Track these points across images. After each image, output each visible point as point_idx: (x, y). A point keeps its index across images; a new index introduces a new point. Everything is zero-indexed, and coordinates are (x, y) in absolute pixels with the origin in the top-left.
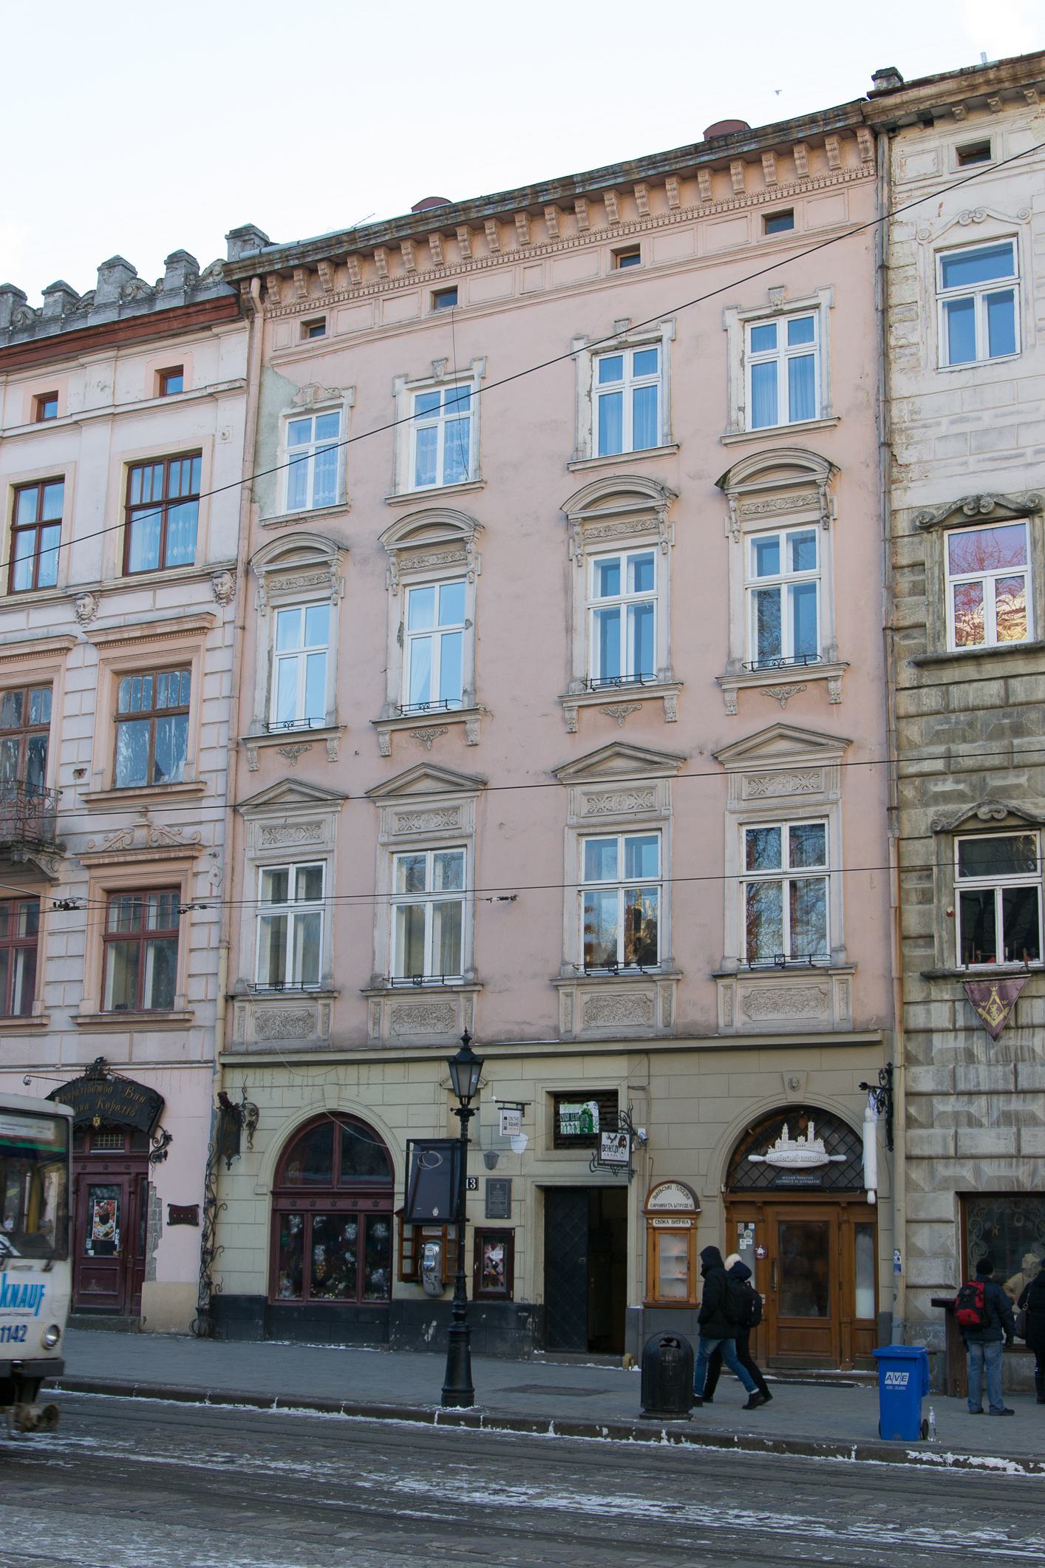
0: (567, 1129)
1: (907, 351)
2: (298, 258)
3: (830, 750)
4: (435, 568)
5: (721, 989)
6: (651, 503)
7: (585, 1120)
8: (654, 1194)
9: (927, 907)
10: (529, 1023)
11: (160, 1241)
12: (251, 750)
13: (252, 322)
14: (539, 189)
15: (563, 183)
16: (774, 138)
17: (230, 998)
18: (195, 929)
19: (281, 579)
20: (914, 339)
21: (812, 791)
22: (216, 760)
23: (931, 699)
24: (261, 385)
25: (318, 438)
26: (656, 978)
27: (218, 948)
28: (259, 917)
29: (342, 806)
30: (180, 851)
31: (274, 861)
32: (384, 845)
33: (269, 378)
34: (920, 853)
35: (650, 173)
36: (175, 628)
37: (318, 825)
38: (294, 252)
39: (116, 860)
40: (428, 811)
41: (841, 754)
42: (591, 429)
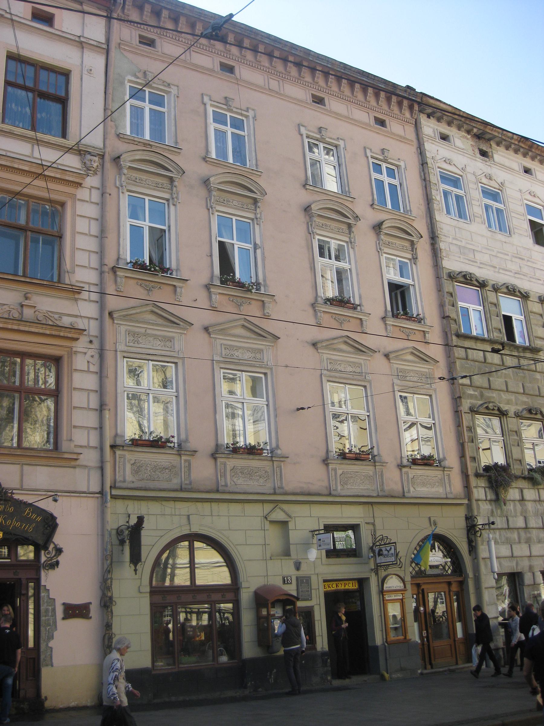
0: (339, 546)
6: (350, 221)
11: (55, 634)
14: (294, 47)
16: (391, 88)
19: (136, 175)
30: (70, 332)
35: (342, 71)
36: (58, 176)
37: (170, 339)
39: (10, 326)
40: (243, 348)
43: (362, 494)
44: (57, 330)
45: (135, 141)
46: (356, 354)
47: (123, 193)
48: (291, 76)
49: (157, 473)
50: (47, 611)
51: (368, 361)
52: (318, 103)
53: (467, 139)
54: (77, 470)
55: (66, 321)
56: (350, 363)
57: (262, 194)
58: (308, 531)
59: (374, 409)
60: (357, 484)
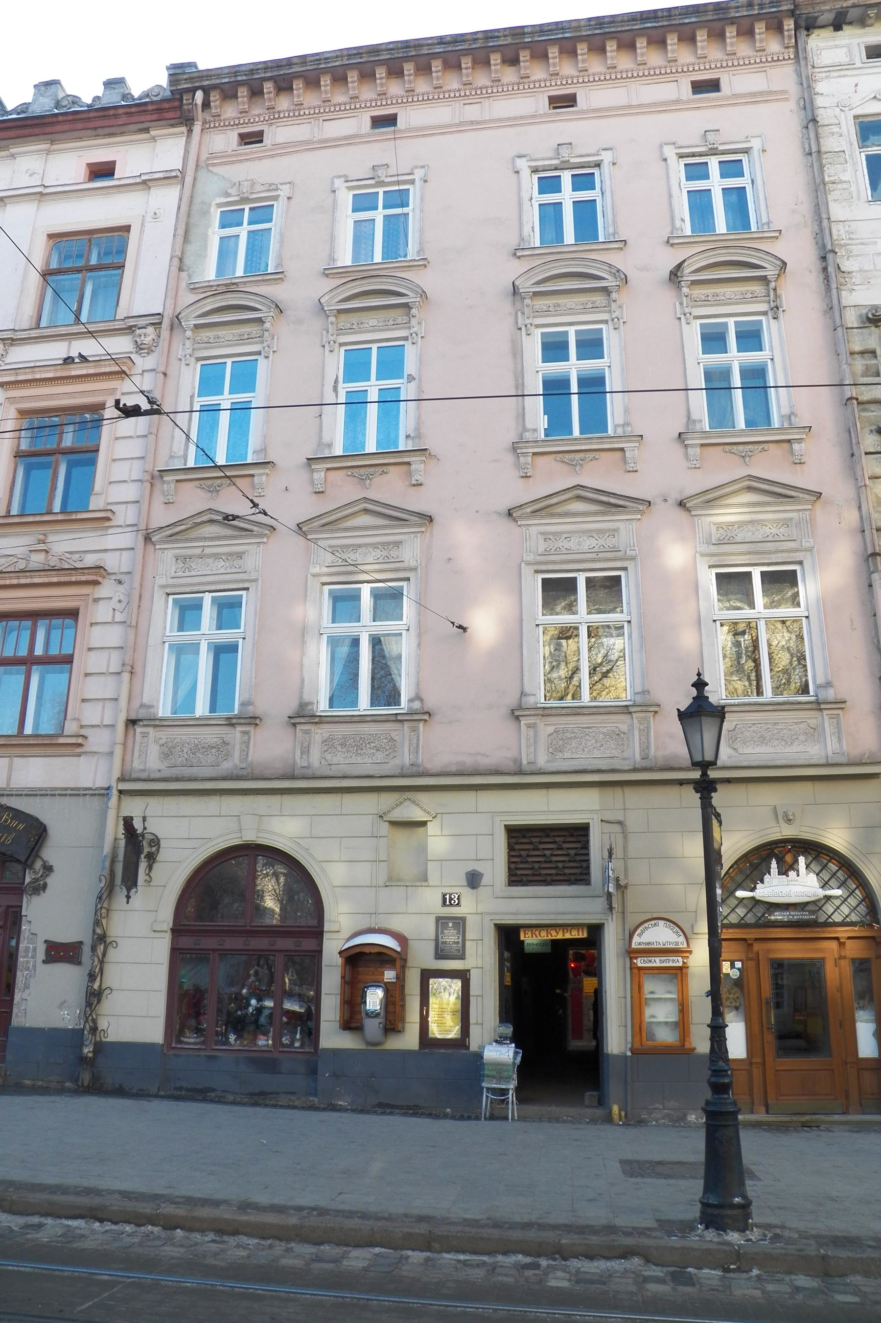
1: (839, 186)
2: (246, 75)
3: (800, 503)
4: (374, 329)
8: (638, 931)
10: (483, 755)
12: (168, 482)
13: (190, 131)
14: (490, 35)
15: (512, 32)
17: (132, 723)
18: (92, 654)
19: (208, 334)
22: (130, 492)
24: (195, 179)
25: (250, 223)
27: (119, 673)
28: (167, 645)
29: (268, 538)
31: (188, 589)
32: (314, 576)
33: (202, 174)
35: (597, 32)
37: (240, 555)
38: (244, 68)
40: (366, 545)
41: (810, 507)
42: (533, 228)
43: (595, 767)
44: (67, 575)
45: (211, 286)
46: (603, 513)
47: (187, 365)
48: (503, 85)
49: (198, 754)
50: (27, 950)
52: (572, 106)
54: (82, 759)
55: (90, 560)
56: (589, 533)
57: (416, 292)
59: (639, 607)
60: (586, 750)
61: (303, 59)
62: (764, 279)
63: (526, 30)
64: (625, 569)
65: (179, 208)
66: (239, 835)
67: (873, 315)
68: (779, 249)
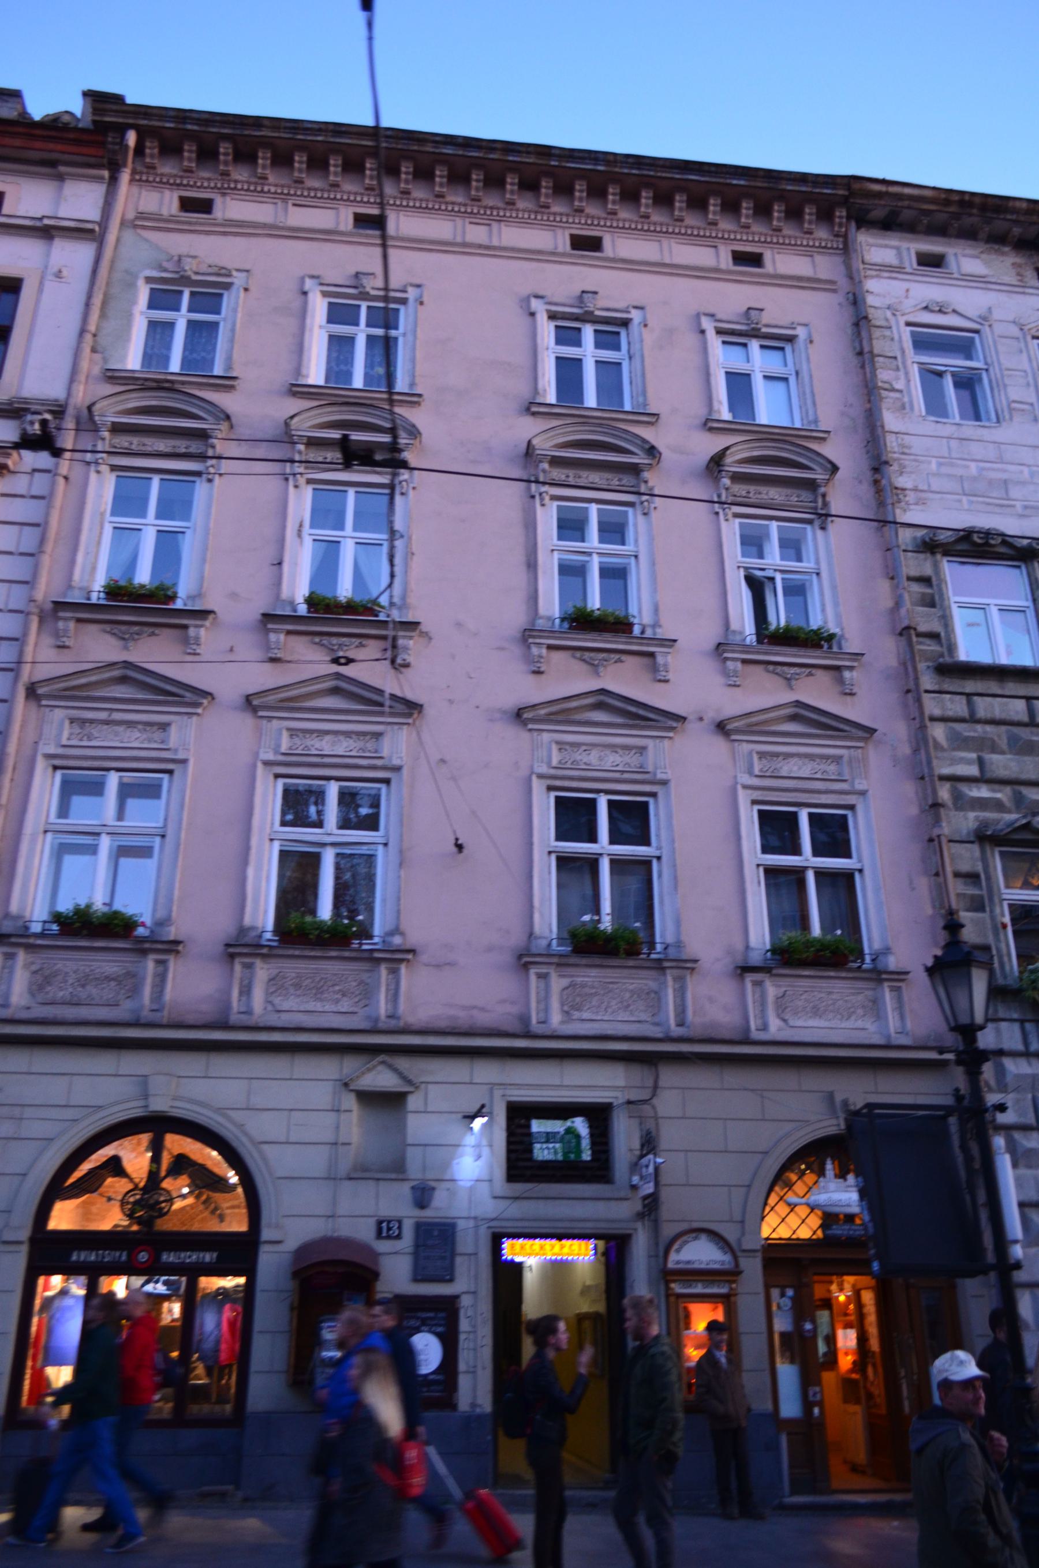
0: (542, 1152)
1: (892, 394)
5: (749, 985)
7: (569, 1142)
8: (676, 1246)
9: (980, 915)
10: (482, 1009)
14: (510, 147)
20: (899, 385)
21: (833, 777)
23: (957, 706)
24: (118, 240)
26: (667, 964)
29: (204, 709)
32: (267, 763)
34: (967, 858)
35: (634, 171)
40: (336, 733)
48: (518, 210)
51: (666, 742)
53: (1003, 254)
58: (460, 1116)
61: (276, 123)
62: (811, 485)
63: (553, 151)
64: (654, 795)
65: (94, 272)
66: (141, 1103)
67: (931, 539)
68: (828, 450)
